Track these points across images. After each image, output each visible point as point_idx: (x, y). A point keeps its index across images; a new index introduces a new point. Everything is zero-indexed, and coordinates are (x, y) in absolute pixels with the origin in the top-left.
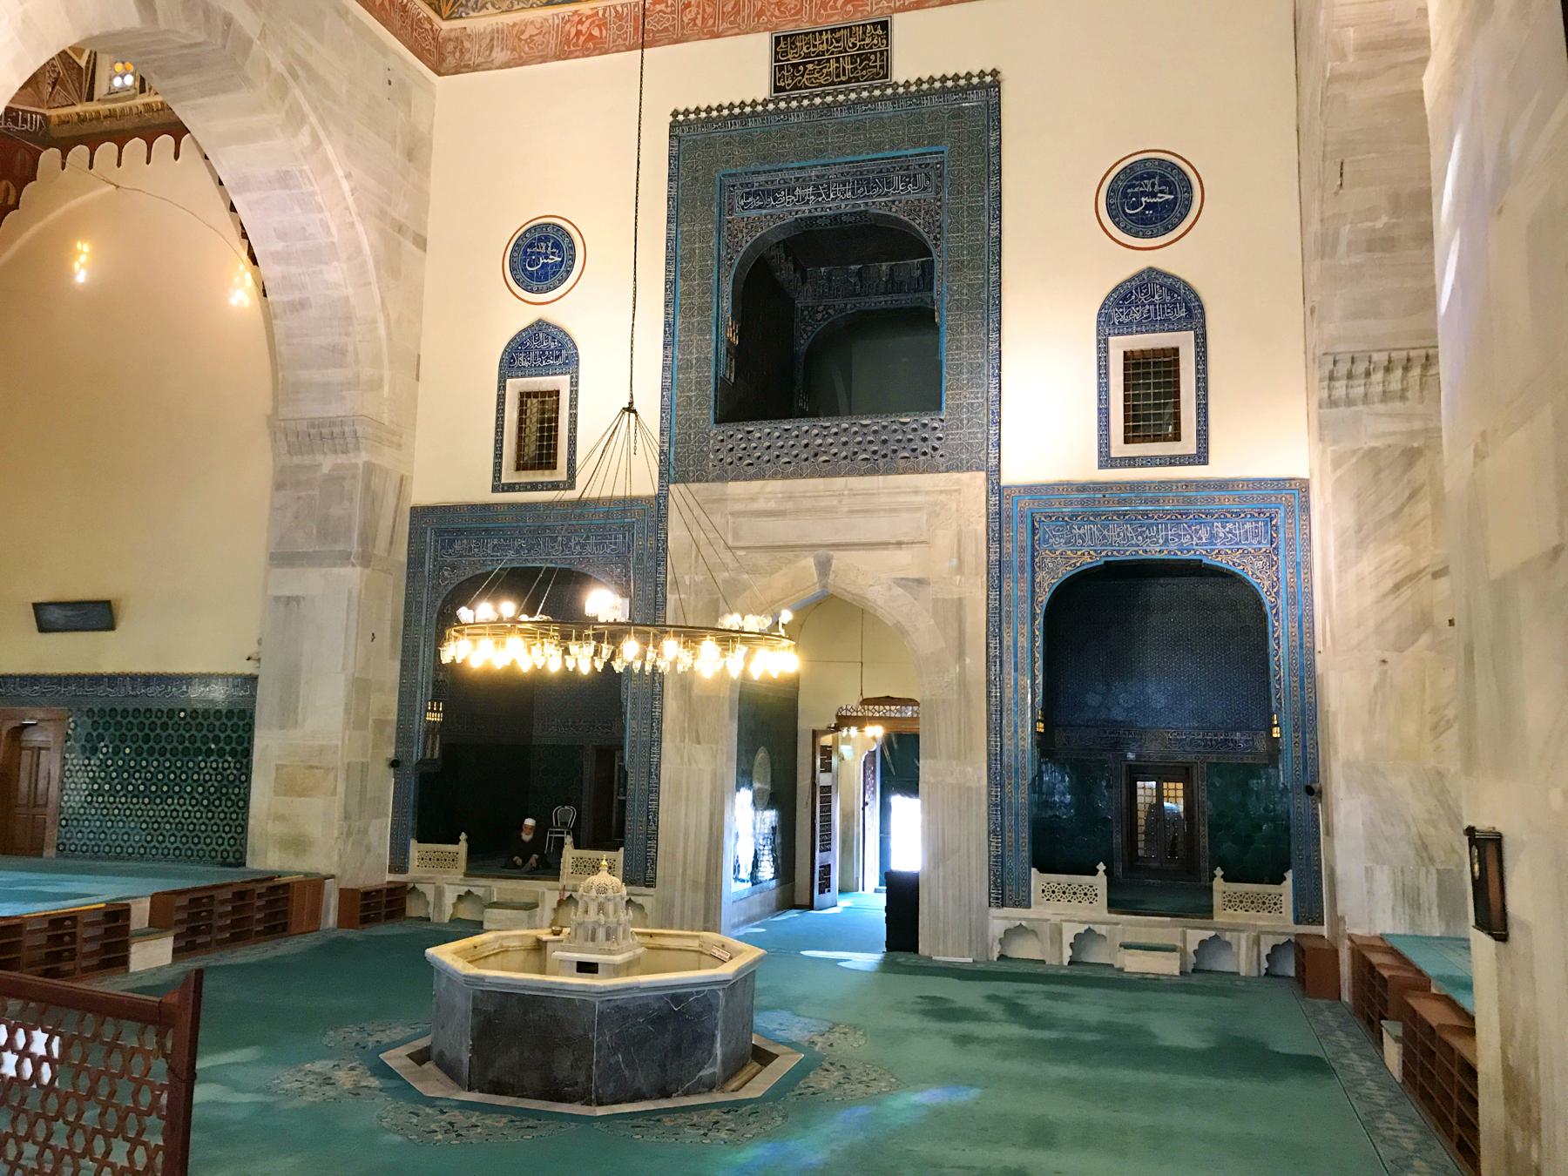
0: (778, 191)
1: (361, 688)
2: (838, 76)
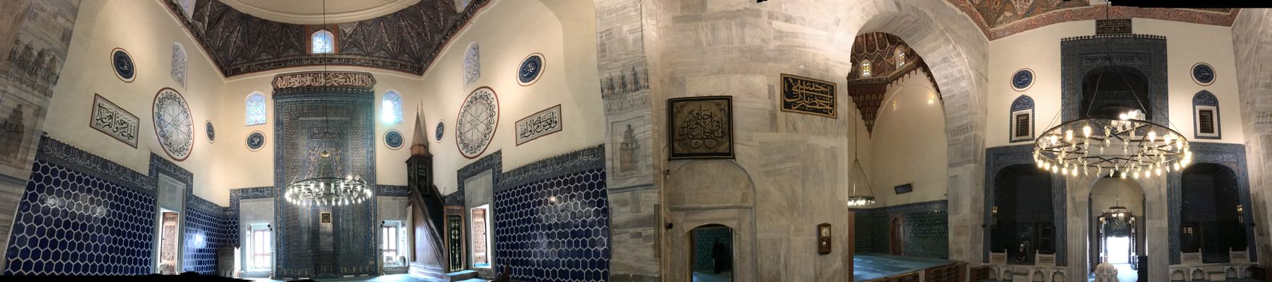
1: (975, 200)
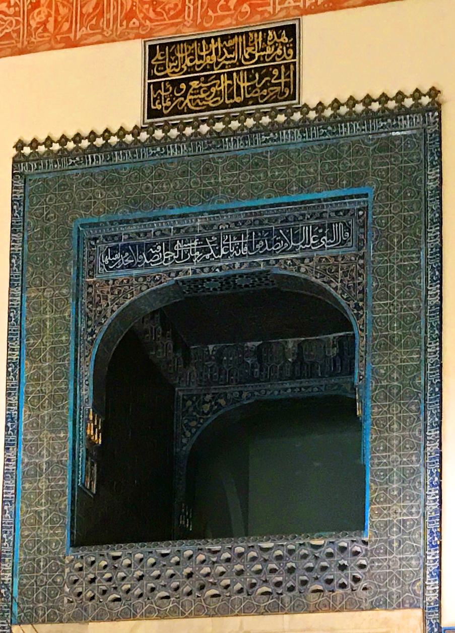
0: (153, 245)
2: (231, 96)
